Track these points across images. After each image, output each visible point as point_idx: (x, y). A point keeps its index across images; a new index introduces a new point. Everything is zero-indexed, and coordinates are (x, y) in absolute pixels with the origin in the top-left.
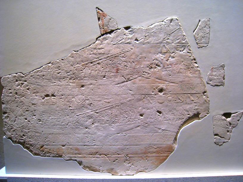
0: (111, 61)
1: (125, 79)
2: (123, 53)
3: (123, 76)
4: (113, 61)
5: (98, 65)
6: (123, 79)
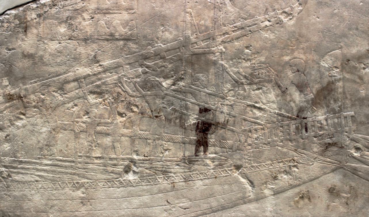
0: (169, 81)
1: (251, 183)
3: (238, 167)
4: (182, 79)
5: (92, 99)
6: (237, 181)
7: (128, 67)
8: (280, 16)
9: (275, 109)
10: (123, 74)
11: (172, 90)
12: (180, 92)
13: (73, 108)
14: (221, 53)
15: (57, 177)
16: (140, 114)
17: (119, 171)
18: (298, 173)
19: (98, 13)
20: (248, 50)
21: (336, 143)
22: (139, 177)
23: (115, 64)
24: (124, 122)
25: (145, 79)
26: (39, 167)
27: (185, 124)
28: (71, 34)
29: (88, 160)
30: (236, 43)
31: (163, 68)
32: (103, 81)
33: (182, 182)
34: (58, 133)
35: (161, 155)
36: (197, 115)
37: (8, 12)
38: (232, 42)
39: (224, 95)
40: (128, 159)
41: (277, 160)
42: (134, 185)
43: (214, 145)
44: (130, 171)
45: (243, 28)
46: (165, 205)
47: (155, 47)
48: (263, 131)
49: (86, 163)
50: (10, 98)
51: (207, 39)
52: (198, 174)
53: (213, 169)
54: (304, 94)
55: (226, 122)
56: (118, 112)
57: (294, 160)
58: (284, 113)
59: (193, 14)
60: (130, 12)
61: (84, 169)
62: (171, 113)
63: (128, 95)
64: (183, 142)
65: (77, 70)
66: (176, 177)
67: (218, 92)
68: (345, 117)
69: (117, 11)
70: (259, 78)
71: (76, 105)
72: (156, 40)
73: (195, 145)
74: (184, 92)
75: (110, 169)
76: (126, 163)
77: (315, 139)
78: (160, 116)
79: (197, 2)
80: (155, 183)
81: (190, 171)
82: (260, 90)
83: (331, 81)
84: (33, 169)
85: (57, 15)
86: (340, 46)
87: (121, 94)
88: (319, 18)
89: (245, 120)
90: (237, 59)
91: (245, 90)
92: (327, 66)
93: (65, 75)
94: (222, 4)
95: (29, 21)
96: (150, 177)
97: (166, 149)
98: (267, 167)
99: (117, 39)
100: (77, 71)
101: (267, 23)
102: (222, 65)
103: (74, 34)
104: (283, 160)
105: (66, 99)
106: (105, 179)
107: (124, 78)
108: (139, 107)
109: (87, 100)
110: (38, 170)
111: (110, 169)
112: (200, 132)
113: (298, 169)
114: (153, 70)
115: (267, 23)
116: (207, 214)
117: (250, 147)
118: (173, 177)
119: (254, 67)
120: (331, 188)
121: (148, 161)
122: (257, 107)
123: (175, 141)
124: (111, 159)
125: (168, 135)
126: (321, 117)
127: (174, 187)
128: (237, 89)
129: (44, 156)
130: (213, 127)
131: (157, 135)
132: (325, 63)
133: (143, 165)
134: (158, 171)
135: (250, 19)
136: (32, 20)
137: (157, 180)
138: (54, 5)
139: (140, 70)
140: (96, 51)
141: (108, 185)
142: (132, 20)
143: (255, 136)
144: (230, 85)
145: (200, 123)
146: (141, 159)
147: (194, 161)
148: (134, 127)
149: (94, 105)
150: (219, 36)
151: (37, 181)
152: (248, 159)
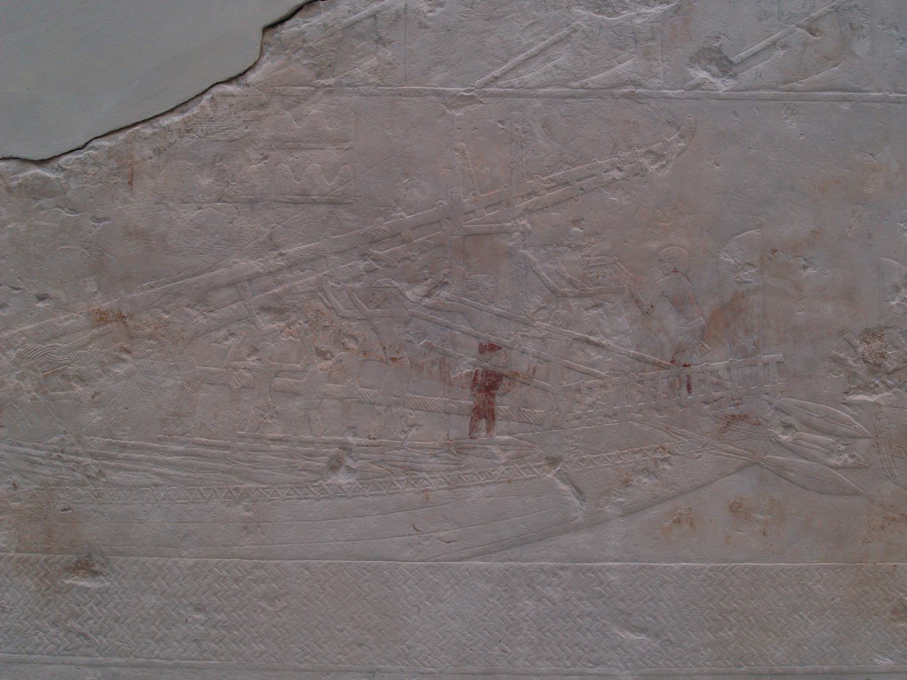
0: (420, 289)
2: (557, 204)
3: (553, 462)
5: (266, 323)
7: (338, 258)
8: (643, 160)
9: (630, 347)
10: (327, 272)
11: (424, 306)
12: (441, 310)
13: (226, 339)
14: (523, 233)
15: (195, 478)
16: (361, 354)
17: (318, 467)
18: (670, 474)
19: (277, 148)
20: (578, 227)
21: (746, 416)
22: (358, 480)
23: (311, 252)
24: (329, 370)
25: (371, 284)
26: (159, 458)
27: (449, 376)
28: (222, 190)
29: (257, 445)
30: (554, 214)
31: (407, 262)
32: (287, 286)
33: (443, 489)
34: (196, 391)
35: (403, 437)
36: (473, 357)
37: (96, 143)
38: (546, 212)
39: (528, 317)
40: (336, 443)
41: (631, 447)
42: (348, 495)
43: (507, 418)
44: (340, 467)
45: (567, 183)
46: (410, 535)
47: (391, 218)
48: (604, 391)
49: (252, 451)
50: (101, 318)
51: (496, 204)
52: (475, 474)
53: (505, 464)
54: (686, 318)
55: (531, 371)
56: (316, 349)
57: (663, 448)
58: (645, 355)
59: (467, 153)
60: (341, 146)
61: (250, 461)
62: (423, 353)
63: (337, 315)
64: (447, 411)
65: (235, 263)
66: (431, 480)
67: (517, 312)
68: (766, 364)
69: (314, 145)
70: (599, 284)
71: (232, 335)
72: (394, 205)
73: (470, 418)
74: (450, 311)
75: (301, 462)
76: (334, 450)
77: (706, 407)
78: (400, 358)
79: (476, 128)
80: (390, 492)
81: (460, 469)
82: (600, 309)
83: (740, 291)
84: (149, 461)
85: (194, 151)
86: (758, 223)
87: (323, 314)
88: (718, 165)
89: (569, 368)
90: (555, 245)
91: (569, 308)
92: (732, 261)
93: (212, 274)
94: (526, 132)
95: (137, 163)
96: (380, 480)
97: (412, 424)
98: (611, 461)
99: (315, 203)
100: (235, 265)
101: (616, 174)
102: (525, 257)
103: (228, 191)
104: (643, 448)
105: (213, 323)
106: (290, 483)
107: (329, 282)
108: (359, 339)
109: (255, 325)
110: (158, 463)
111: (301, 462)
112: (480, 391)
113: (671, 465)
114: (386, 266)
115: (616, 174)
116: (491, 553)
117: (577, 422)
118: (425, 479)
119: (589, 262)
120: (734, 503)
121: (376, 448)
122: (593, 341)
123: (429, 409)
124: (303, 443)
125: (416, 396)
126: (719, 365)
127: (428, 498)
128: (554, 306)
129: (170, 435)
130: (505, 381)
131: (396, 396)
132: (728, 256)
133: (366, 455)
134: (397, 466)
135: (582, 164)
136: (144, 160)
137: (395, 485)
138: (188, 131)
139: (362, 265)
140: (272, 225)
141: (298, 494)
142: (346, 164)
143: (589, 399)
144: (539, 298)
145: (480, 373)
146: (363, 443)
147: (468, 448)
148: (349, 380)
149: (269, 334)
150: (520, 199)
151: (156, 485)
152: (573, 446)
